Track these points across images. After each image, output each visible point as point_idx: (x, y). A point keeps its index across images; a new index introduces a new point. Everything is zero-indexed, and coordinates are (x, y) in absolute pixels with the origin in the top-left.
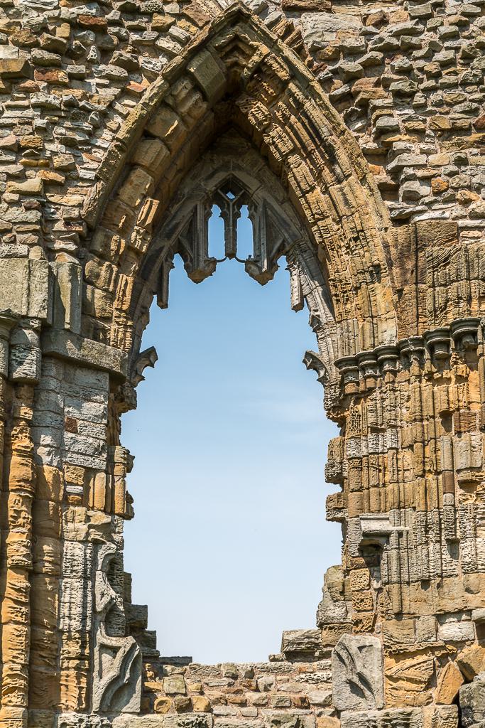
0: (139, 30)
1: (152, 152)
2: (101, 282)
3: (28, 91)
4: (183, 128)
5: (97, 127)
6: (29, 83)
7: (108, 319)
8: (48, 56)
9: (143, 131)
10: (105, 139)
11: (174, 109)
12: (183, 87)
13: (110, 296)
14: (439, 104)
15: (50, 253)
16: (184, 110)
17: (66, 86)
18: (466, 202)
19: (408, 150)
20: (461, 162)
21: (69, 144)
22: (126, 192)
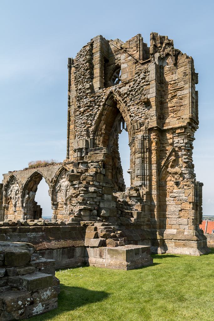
0: (100, 99)
1: (103, 117)
2: (97, 139)
3: (85, 114)
4: (108, 112)
5: (94, 117)
6: (85, 113)
7: (99, 145)
8: (87, 108)
9: (101, 115)
10: (96, 118)
11: (106, 110)
12: (106, 106)
13: (99, 141)
14: (136, 99)
15: (89, 137)
16: (107, 110)
17: (90, 111)
18: (139, 115)
19: (132, 109)
20: (138, 109)
21: (91, 120)
22: (100, 125)
